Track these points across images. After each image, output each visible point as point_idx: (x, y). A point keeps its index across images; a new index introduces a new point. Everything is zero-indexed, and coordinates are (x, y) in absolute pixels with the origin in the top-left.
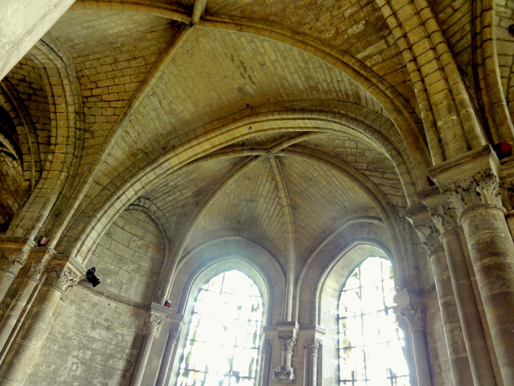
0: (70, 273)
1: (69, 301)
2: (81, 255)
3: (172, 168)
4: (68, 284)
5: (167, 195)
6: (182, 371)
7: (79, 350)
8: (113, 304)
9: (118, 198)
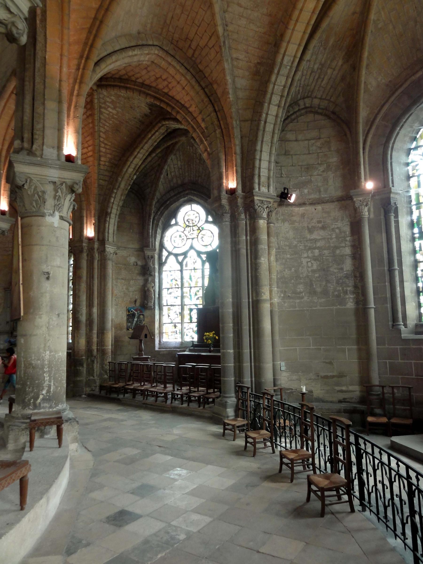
0: (262, 203)
1: (280, 221)
2: (263, 186)
3: (295, 57)
4: (266, 211)
5: (320, 80)
6: (417, 236)
8: (319, 207)
9: (265, 122)
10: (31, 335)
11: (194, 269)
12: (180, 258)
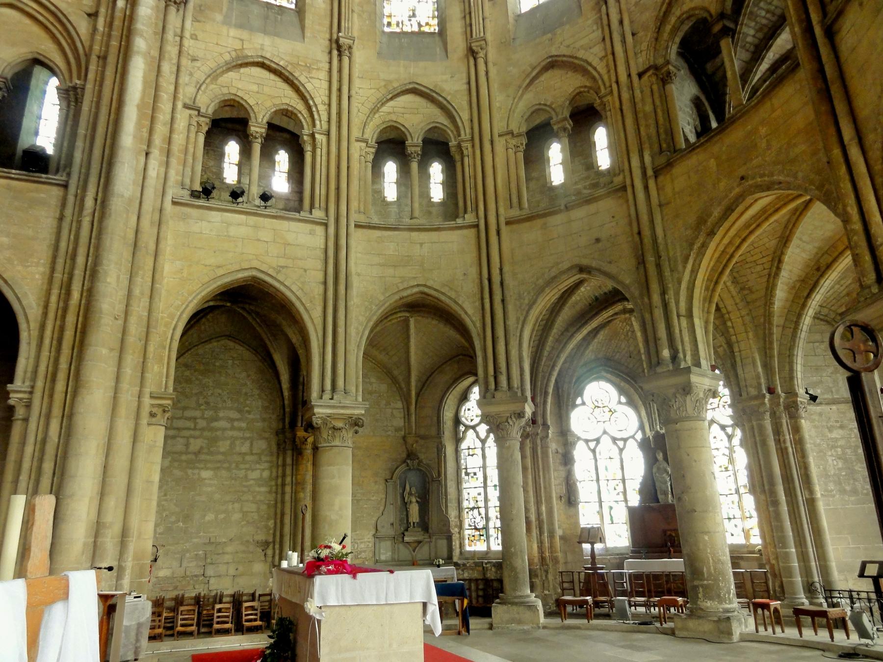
7: (831, 450)
8: (834, 407)
10: (715, 532)
11: (610, 458)
12: (592, 445)
